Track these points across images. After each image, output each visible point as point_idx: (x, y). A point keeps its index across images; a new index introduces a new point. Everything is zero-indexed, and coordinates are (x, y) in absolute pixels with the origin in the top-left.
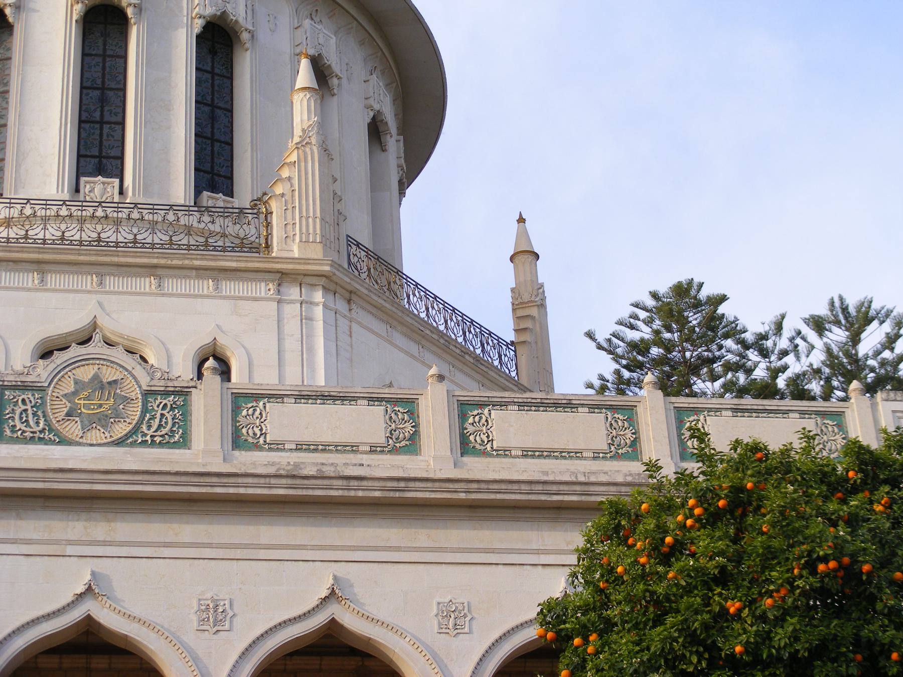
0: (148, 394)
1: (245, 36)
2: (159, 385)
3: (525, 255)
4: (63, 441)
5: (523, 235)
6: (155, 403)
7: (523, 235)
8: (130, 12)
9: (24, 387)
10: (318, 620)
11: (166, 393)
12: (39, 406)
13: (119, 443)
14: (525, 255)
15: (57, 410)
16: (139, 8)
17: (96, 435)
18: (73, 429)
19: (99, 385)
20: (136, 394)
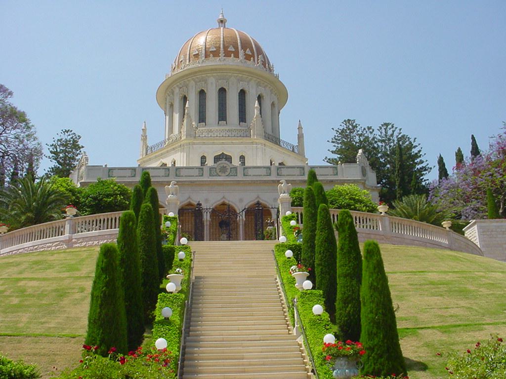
0: (231, 168)
1: (247, 92)
2: (232, 167)
3: (300, 128)
4: (219, 176)
5: (300, 124)
6: (232, 169)
7: (300, 124)
8: (227, 89)
9: (213, 168)
10: (222, 201)
11: (233, 168)
12: (216, 171)
13: (227, 176)
14: (300, 128)
15: (218, 171)
16: (228, 89)
17: (223, 174)
18: (220, 174)
19: (224, 167)
20: (229, 168)
